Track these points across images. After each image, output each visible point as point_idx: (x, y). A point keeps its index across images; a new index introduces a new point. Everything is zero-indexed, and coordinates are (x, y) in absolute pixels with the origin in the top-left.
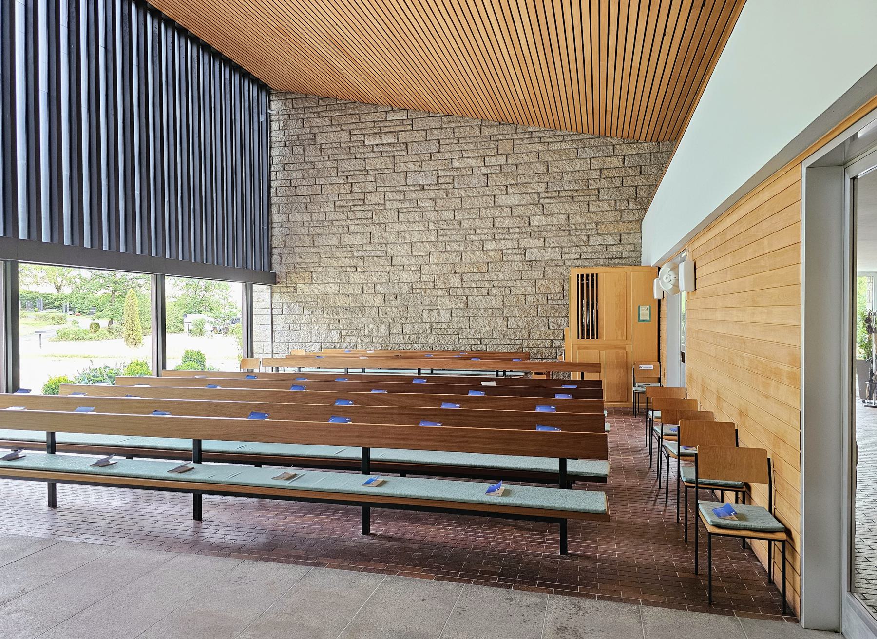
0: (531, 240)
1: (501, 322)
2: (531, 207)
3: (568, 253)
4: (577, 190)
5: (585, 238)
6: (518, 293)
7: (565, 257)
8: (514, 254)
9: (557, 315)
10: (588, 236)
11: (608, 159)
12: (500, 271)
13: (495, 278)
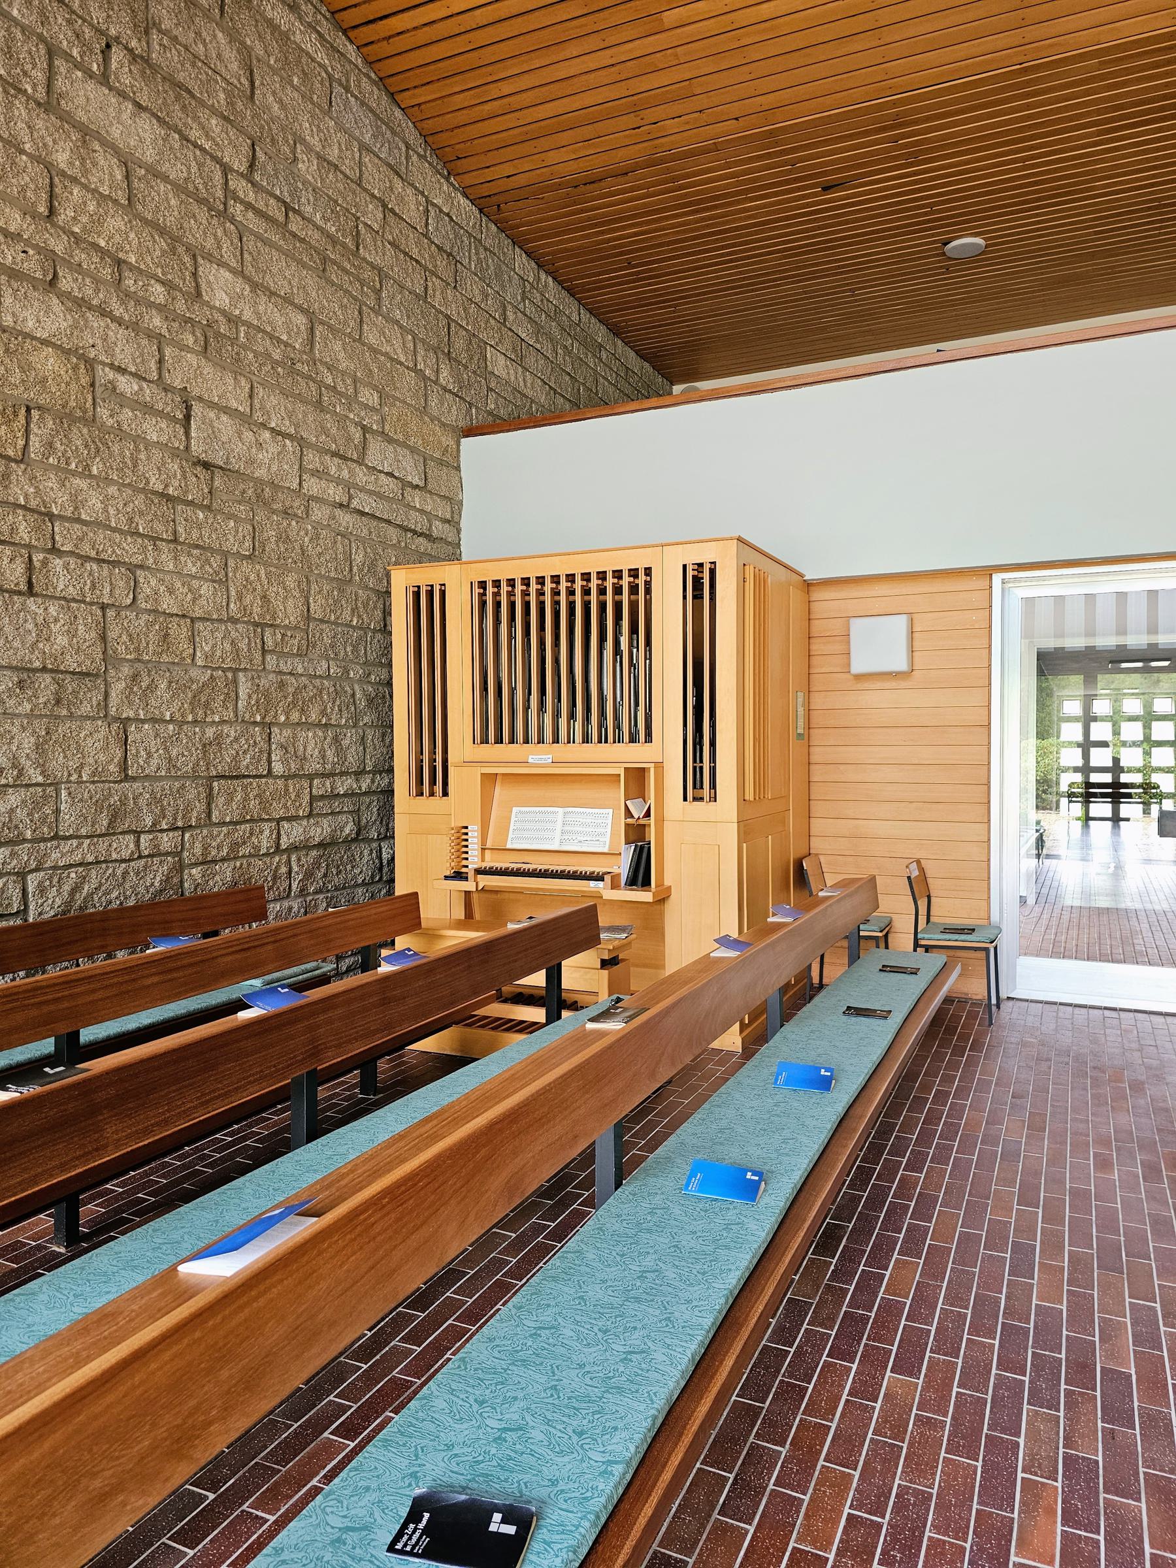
0: (208, 370)
1: (95, 745)
2: (202, 215)
3: (315, 473)
4: (333, 240)
5: (357, 435)
6: (168, 604)
7: (313, 486)
8: (148, 409)
9: (295, 716)
10: (365, 429)
11: (398, 184)
12: (86, 474)
13: (60, 503)
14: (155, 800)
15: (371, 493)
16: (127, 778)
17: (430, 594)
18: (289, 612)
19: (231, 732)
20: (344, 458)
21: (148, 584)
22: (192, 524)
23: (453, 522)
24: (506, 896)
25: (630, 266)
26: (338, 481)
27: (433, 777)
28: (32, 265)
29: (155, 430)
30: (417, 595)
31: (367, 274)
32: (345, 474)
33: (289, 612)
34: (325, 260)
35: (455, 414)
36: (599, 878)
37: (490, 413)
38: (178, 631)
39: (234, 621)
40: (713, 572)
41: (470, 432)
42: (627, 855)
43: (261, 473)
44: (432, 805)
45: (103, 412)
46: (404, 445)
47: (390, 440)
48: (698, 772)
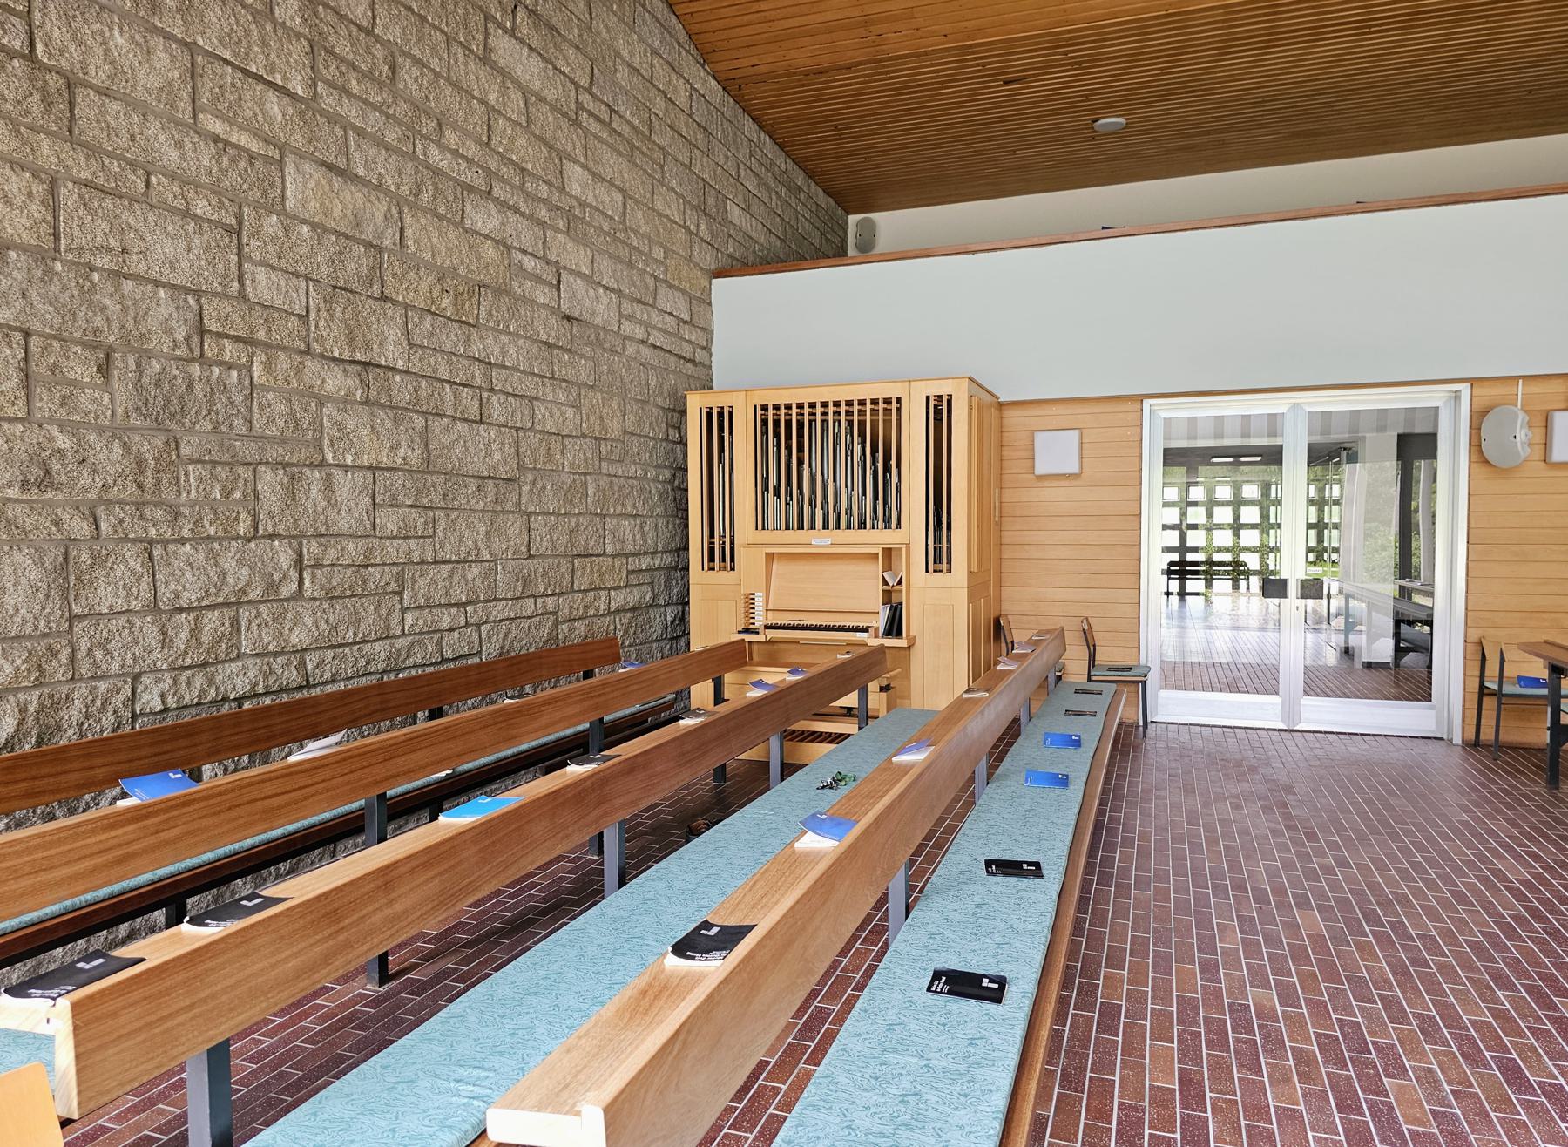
3: (629, 318)
7: (627, 328)
8: (538, 279)
14: (545, 573)
15: (660, 330)
16: (530, 557)
17: (721, 414)
18: (615, 431)
19: (584, 521)
20: (644, 303)
21: (540, 410)
22: (564, 365)
23: (707, 349)
24: (782, 646)
25: (836, 128)
26: (641, 322)
27: (721, 555)
28: (480, 182)
29: (543, 295)
30: (709, 415)
31: (657, 154)
32: (645, 317)
33: (615, 431)
34: (633, 147)
35: (709, 260)
36: (865, 630)
37: (729, 256)
38: (556, 445)
39: (584, 436)
40: (949, 402)
41: (719, 274)
42: (883, 615)
43: (598, 321)
44: (722, 577)
45: (515, 284)
46: (678, 289)
47: (671, 286)
48: (938, 550)
